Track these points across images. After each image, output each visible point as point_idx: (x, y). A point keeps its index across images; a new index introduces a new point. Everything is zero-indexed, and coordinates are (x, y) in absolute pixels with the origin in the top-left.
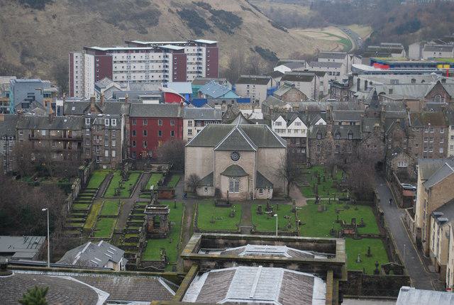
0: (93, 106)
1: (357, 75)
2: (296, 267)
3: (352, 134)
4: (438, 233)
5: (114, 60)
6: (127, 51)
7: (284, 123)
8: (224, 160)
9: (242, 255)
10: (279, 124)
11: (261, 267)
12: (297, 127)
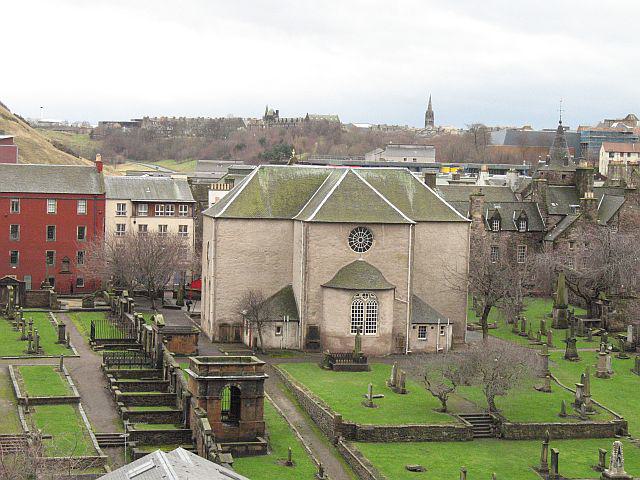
3: (526, 220)
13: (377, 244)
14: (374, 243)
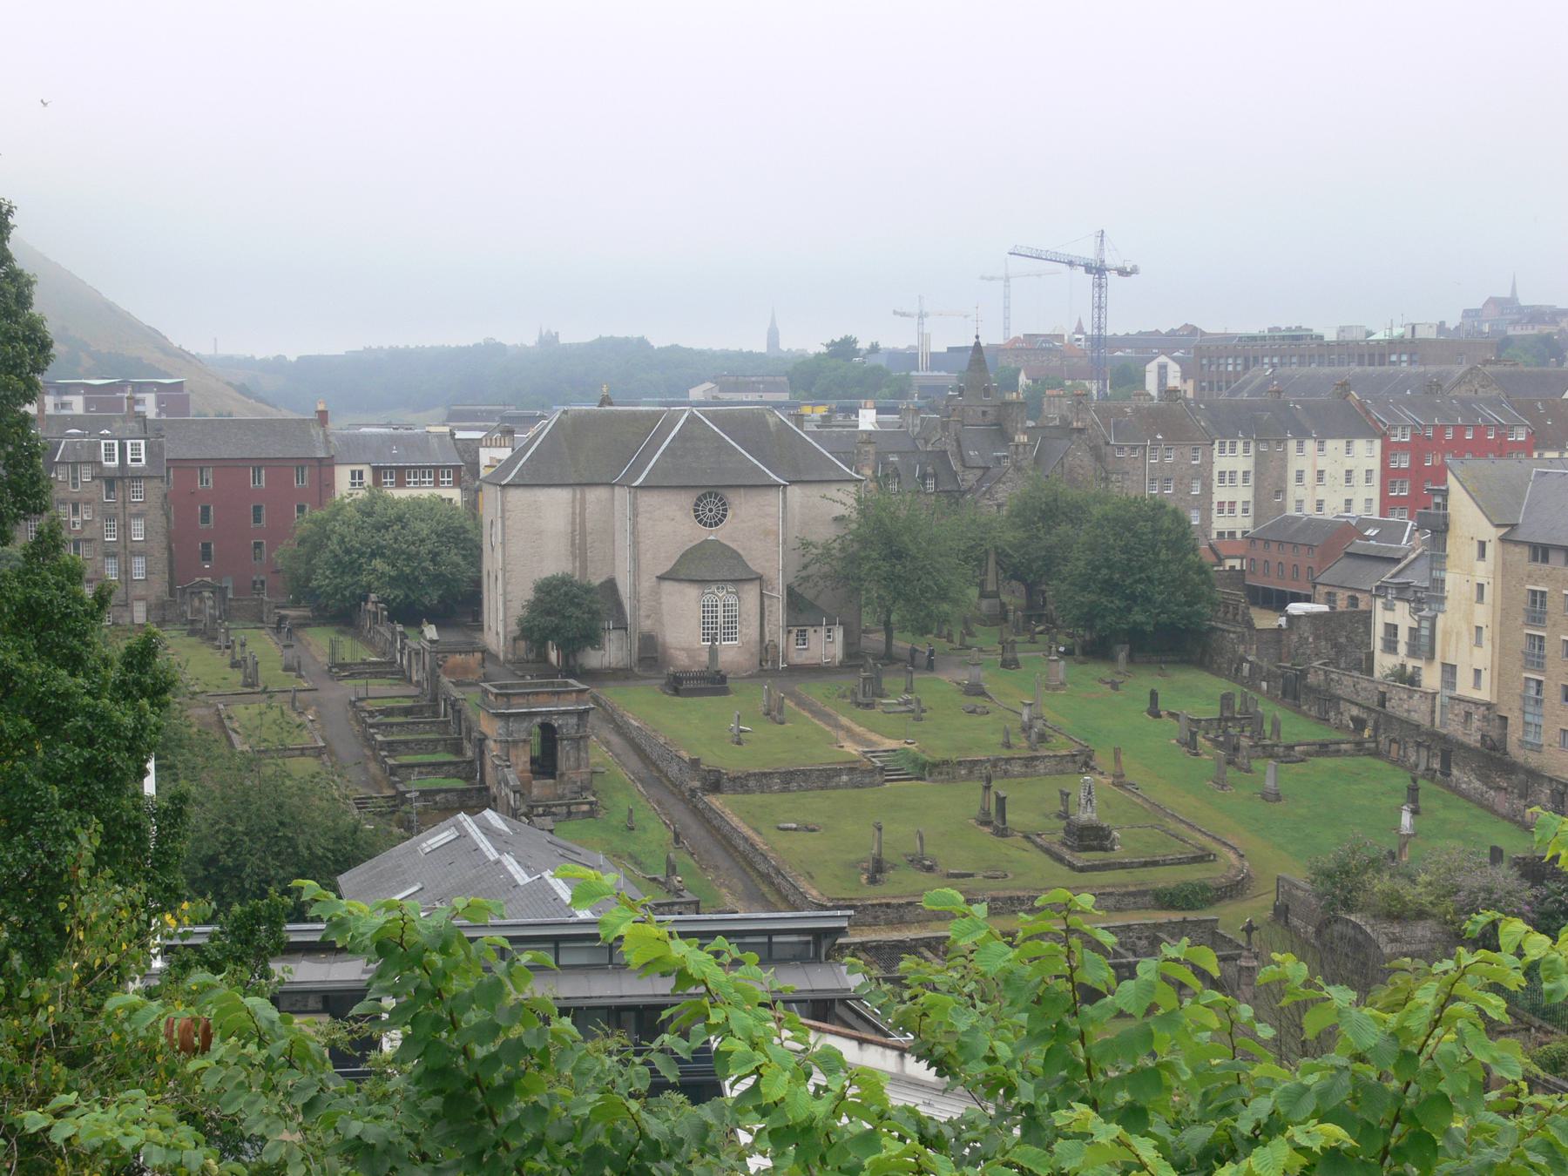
13: (734, 515)
14: (730, 514)
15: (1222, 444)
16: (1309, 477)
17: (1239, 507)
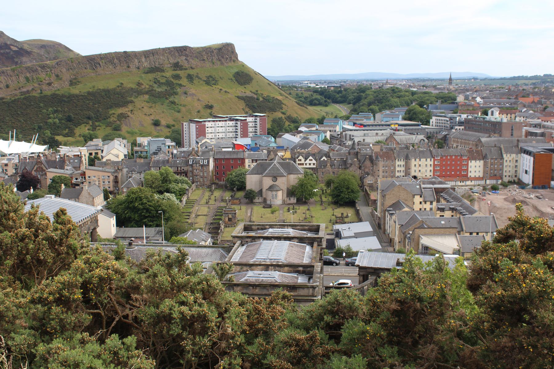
0: (193, 153)
1: (345, 131)
2: (297, 240)
4: (390, 220)
5: (207, 126)
6: (214, 121)
7: (303, 160)
8: (268, 182)
9: (266, 235)
10: (301, 160)
11: (276, 241)
12: (311, 162)
15: (398, 160)
16: (417, 166)
17: (402, 171)
